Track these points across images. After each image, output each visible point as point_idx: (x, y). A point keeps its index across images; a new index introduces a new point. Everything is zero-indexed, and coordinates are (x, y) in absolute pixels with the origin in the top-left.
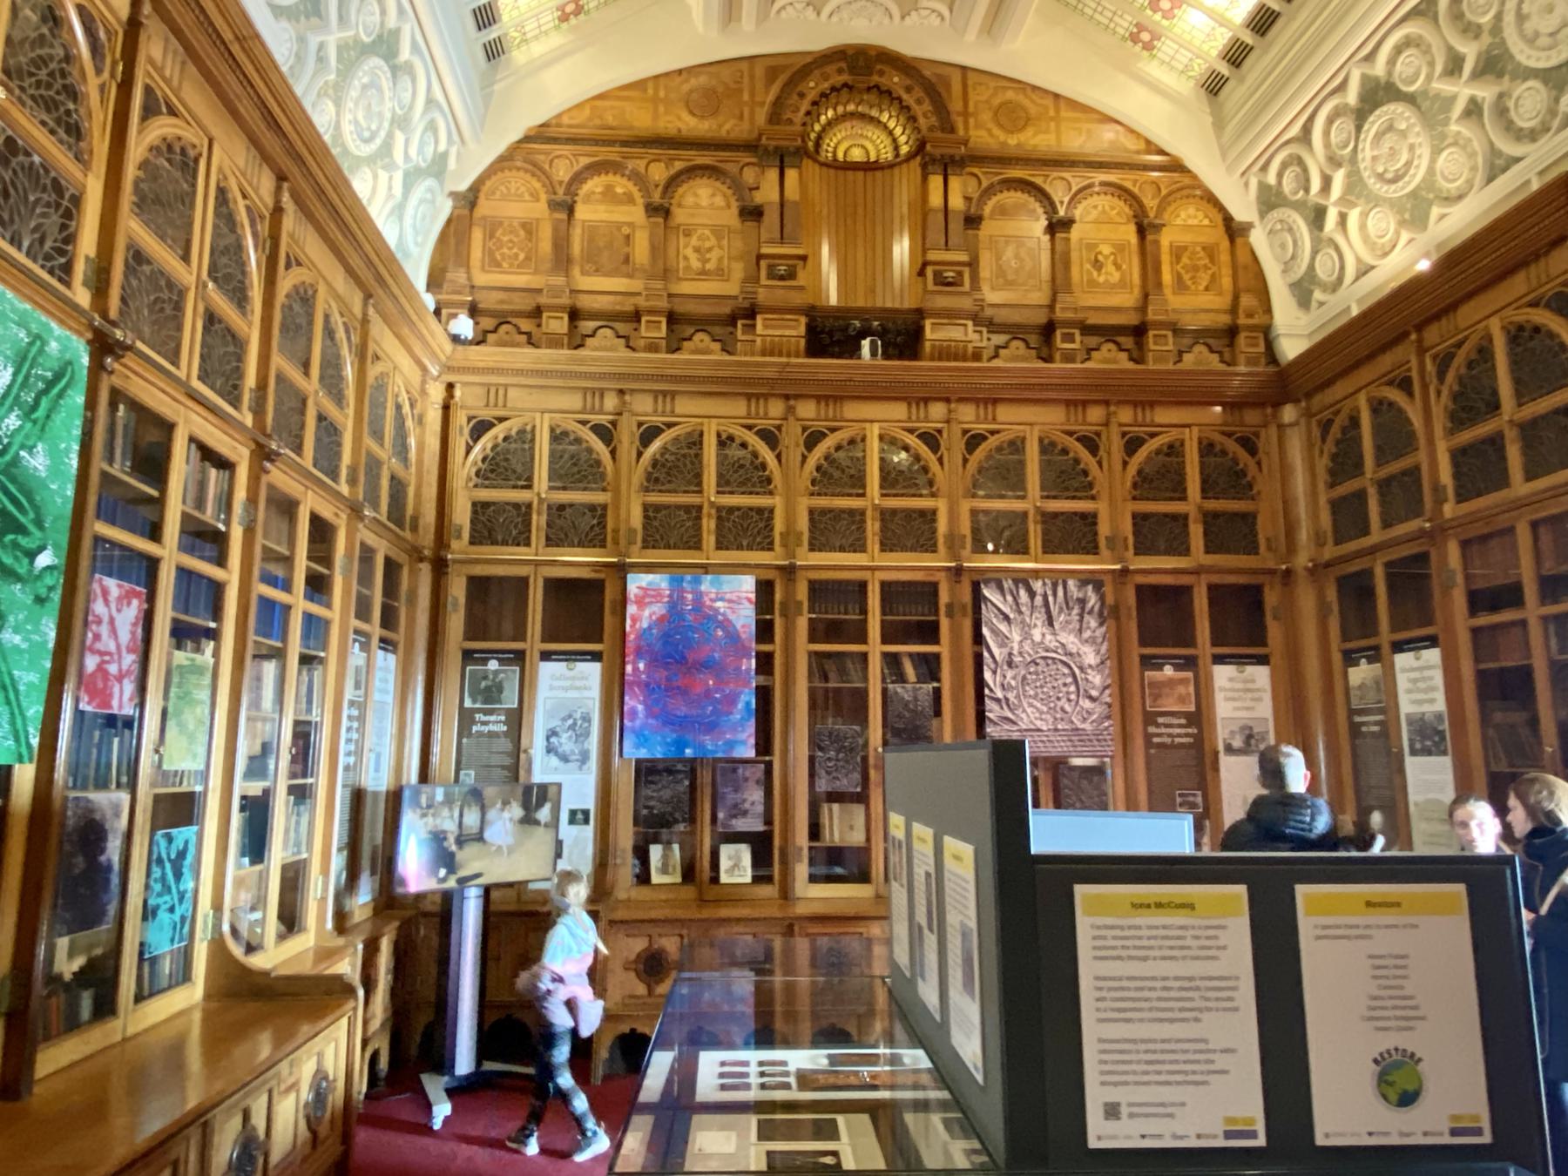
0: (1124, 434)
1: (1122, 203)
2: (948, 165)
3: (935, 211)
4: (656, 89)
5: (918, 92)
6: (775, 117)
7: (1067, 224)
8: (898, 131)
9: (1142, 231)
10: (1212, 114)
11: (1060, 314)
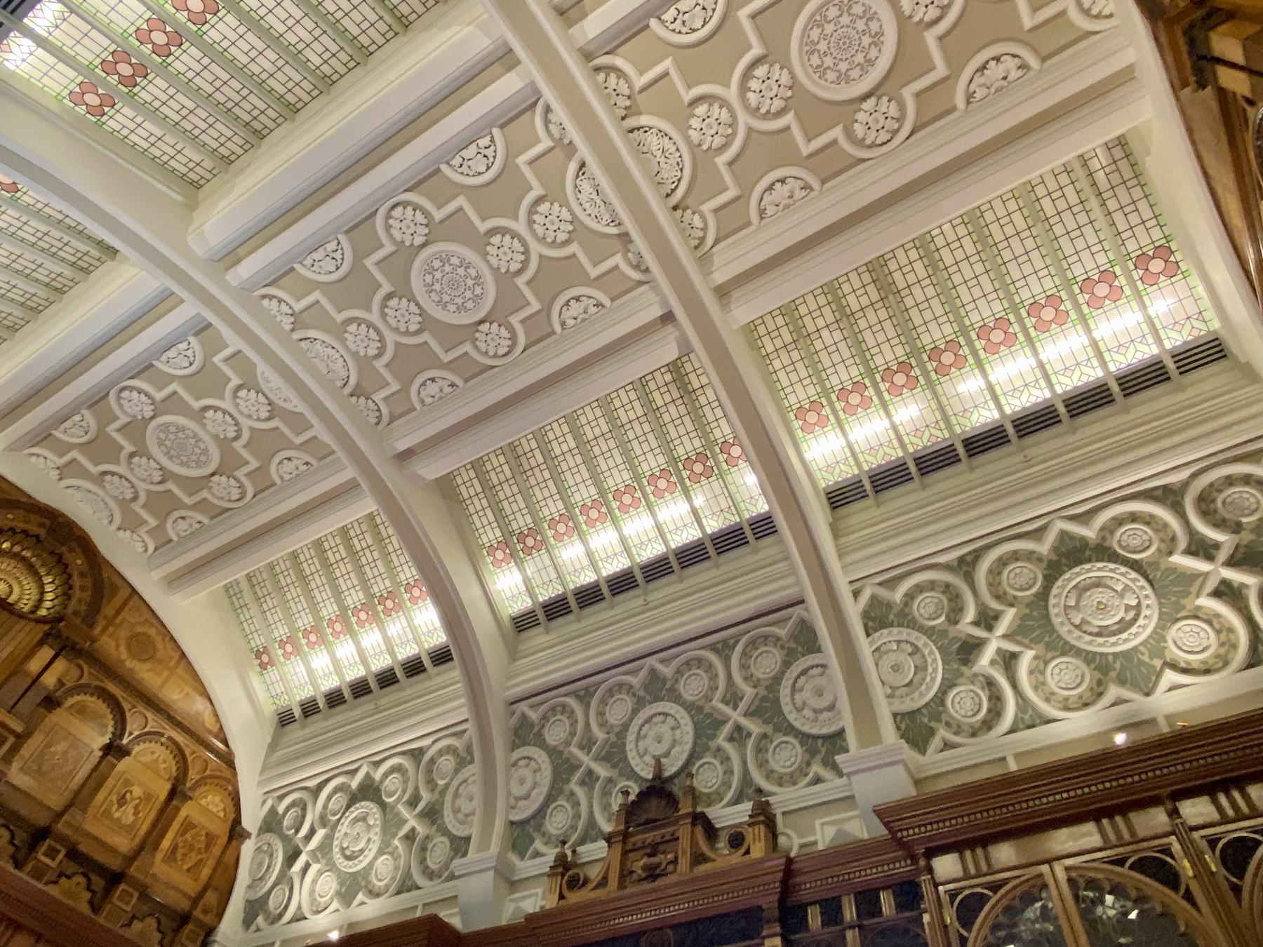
1: (173, 763)
2: (66, 648)
3: (27, 674)
5: (88, 582)
8: (50, 596)
9: (173, 793)
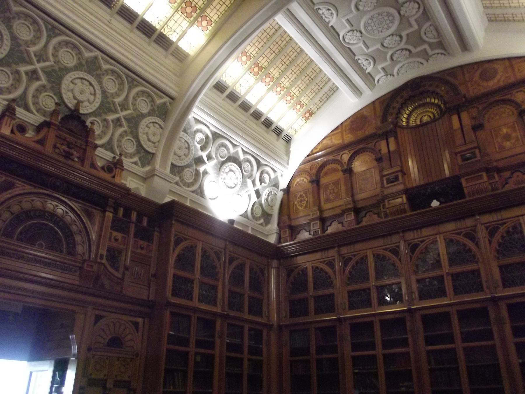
2: (457, 110)
4: (342, 128)
6: (384, 119)
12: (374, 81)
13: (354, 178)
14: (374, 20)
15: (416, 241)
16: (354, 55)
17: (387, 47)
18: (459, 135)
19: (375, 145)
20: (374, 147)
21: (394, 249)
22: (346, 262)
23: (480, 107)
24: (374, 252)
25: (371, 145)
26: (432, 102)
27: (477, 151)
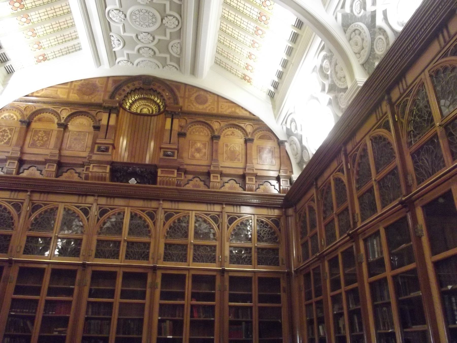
0: (228, 216)
2: (173, 115)
4: (71, 86)
6: (112, 96)
7: (218, 137)
10: (272, 104)
11: (247, 171)
12: (116, 60)
13: (67, 134)
14: (141, 13)
15: (107, 207)
16: (111, 30)
17: (139, 40)
18: (167, 134)
19: (97, 114)
20: (95, 115)
21: (85, 209)
22: (35, 208)
23: (189, 121)
24: (66, 207)
25: (94, 113)
26: (155, 100)
27: (176, 152)
